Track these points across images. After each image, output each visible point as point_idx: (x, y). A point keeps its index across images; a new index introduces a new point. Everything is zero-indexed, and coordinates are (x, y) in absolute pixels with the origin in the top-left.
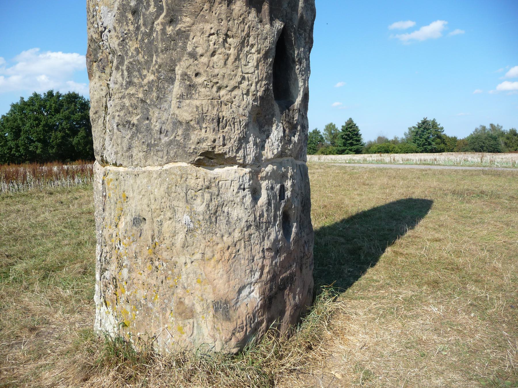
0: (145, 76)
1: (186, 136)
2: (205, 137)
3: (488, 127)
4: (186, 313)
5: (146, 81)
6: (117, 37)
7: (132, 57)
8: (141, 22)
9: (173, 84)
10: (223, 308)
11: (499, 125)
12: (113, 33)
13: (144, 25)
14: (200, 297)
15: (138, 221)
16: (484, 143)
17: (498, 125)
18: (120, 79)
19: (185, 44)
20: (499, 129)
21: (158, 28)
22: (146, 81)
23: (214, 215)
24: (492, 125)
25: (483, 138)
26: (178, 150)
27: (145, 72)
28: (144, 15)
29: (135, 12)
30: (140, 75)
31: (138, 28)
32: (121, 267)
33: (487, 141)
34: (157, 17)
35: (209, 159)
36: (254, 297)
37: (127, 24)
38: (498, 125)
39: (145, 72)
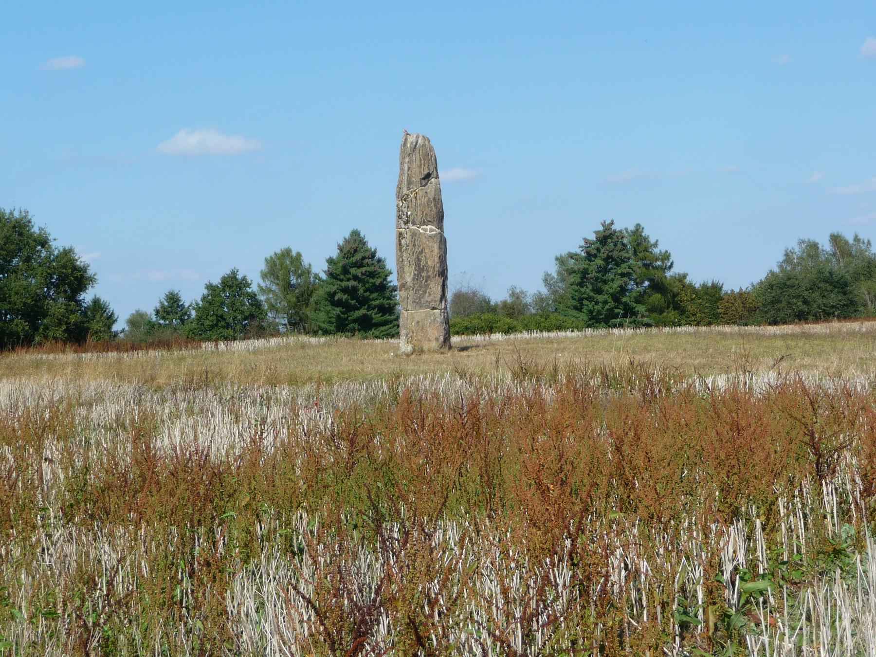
2: (433, 304)
3: (826, 246)
4: (430, 340)
10: (437, 339)
11: (861, 236)
14: (433, 337)
15: (418, 322)
16: (806, 302)
17: (857, 239)
20: (862, 252)
23: (435, 320)
24: (836, 239)
25: (805, 284)
26: (428, 307)
33: (816, 295)
35: (434, 308)
36: (442, 339)
38: (857, 239)
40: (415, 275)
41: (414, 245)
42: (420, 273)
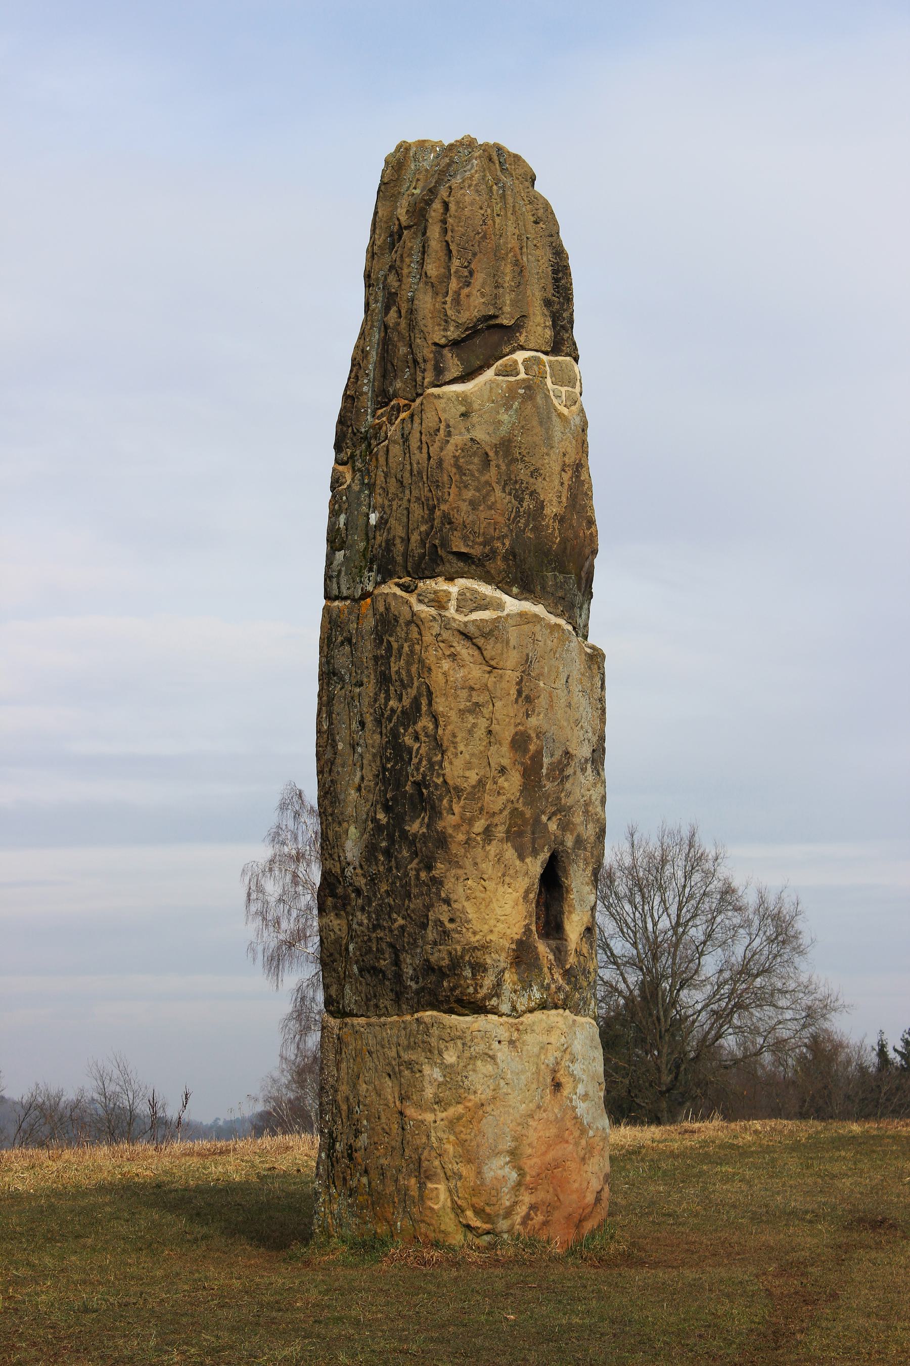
0: (395, 920)
1: (439, 984)
5: (396, 925)
6: (364, 876)
7: (382, 899)
8: (393, 863)
9: (425, 930)
12: (359, 871)
13: (397, 868)
18: (366, 921)
19: (439, 890)
21: (412, 873)
22: (396, 925)
27: (395, 916)
28: (396, 858)
29: (388, 853)
30: (390, 917)
31: (390, 870)
32: (357, 1133)
34: (411, 862)
37: (376, 864)
39: (395, 916)
40: (379, 828)
41: (384, 680)
42: (398, 821)
